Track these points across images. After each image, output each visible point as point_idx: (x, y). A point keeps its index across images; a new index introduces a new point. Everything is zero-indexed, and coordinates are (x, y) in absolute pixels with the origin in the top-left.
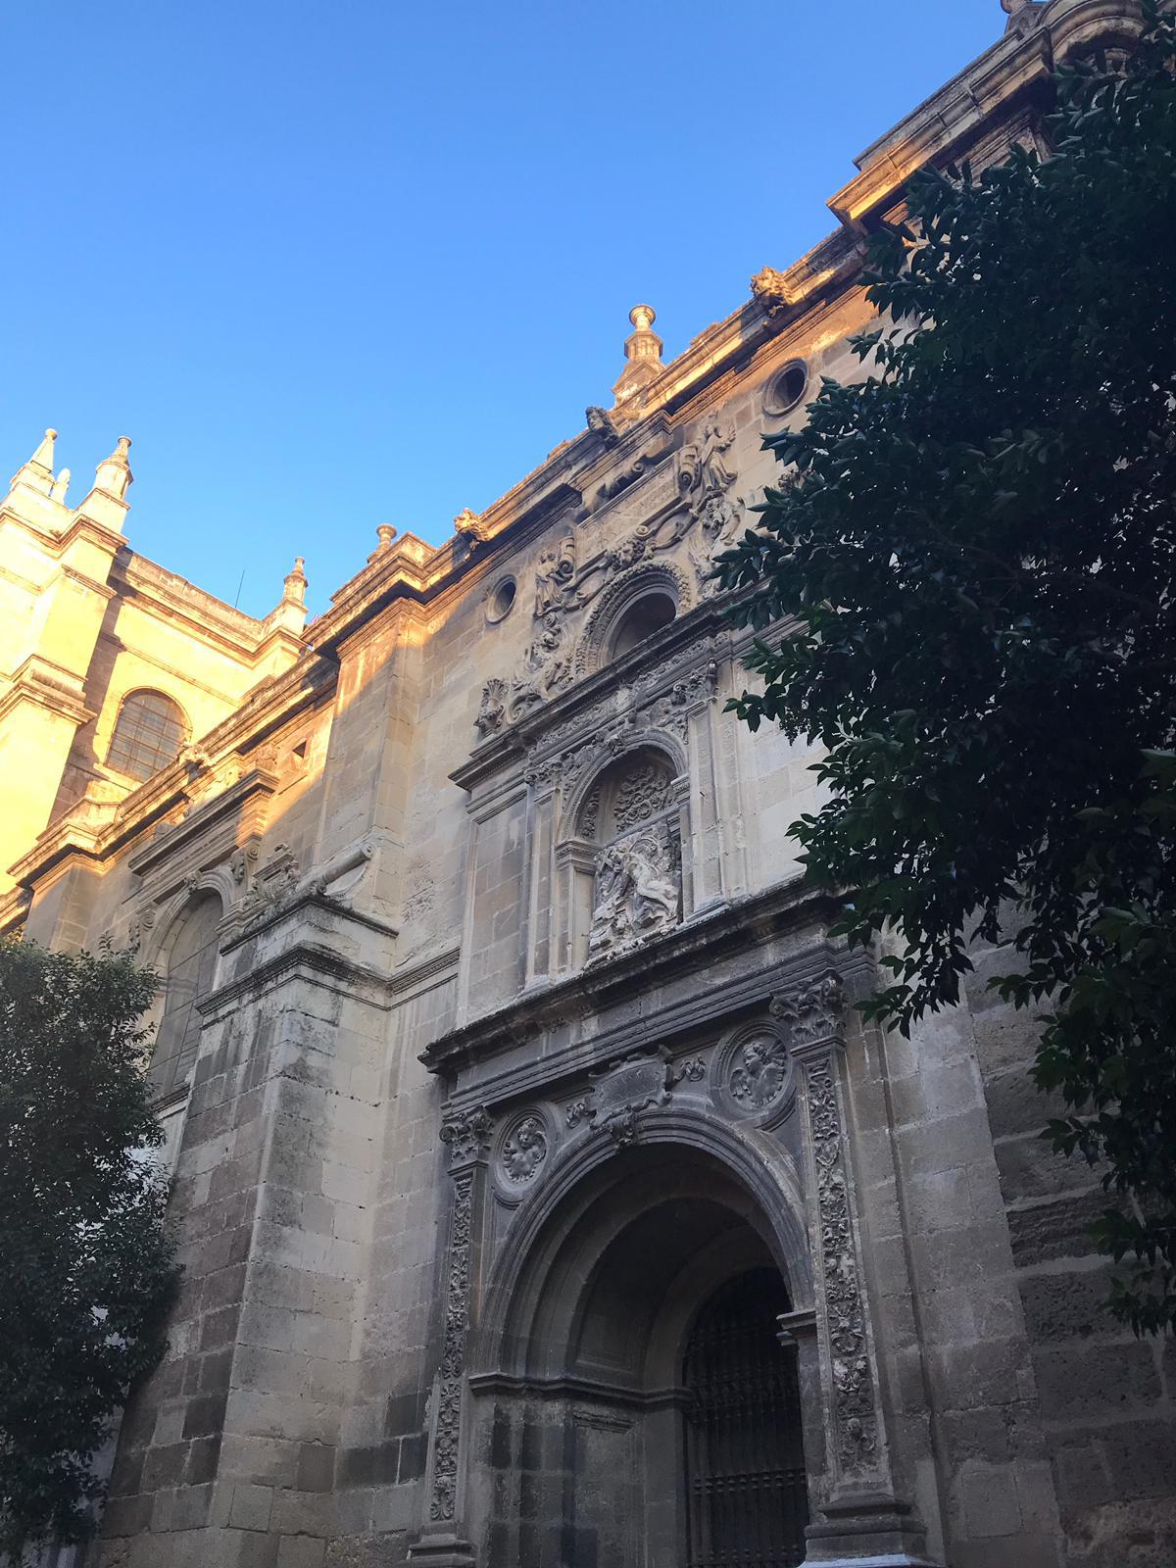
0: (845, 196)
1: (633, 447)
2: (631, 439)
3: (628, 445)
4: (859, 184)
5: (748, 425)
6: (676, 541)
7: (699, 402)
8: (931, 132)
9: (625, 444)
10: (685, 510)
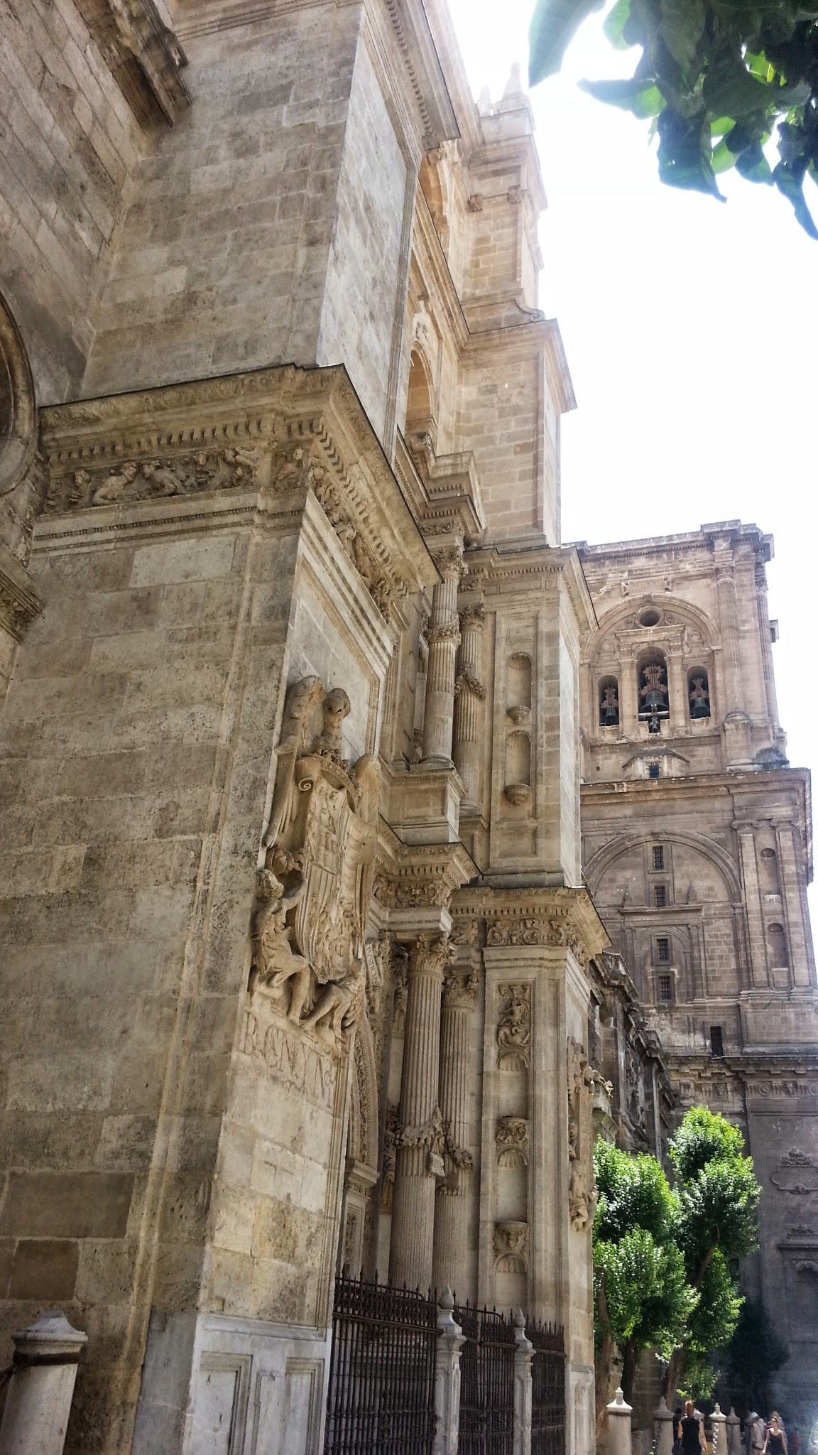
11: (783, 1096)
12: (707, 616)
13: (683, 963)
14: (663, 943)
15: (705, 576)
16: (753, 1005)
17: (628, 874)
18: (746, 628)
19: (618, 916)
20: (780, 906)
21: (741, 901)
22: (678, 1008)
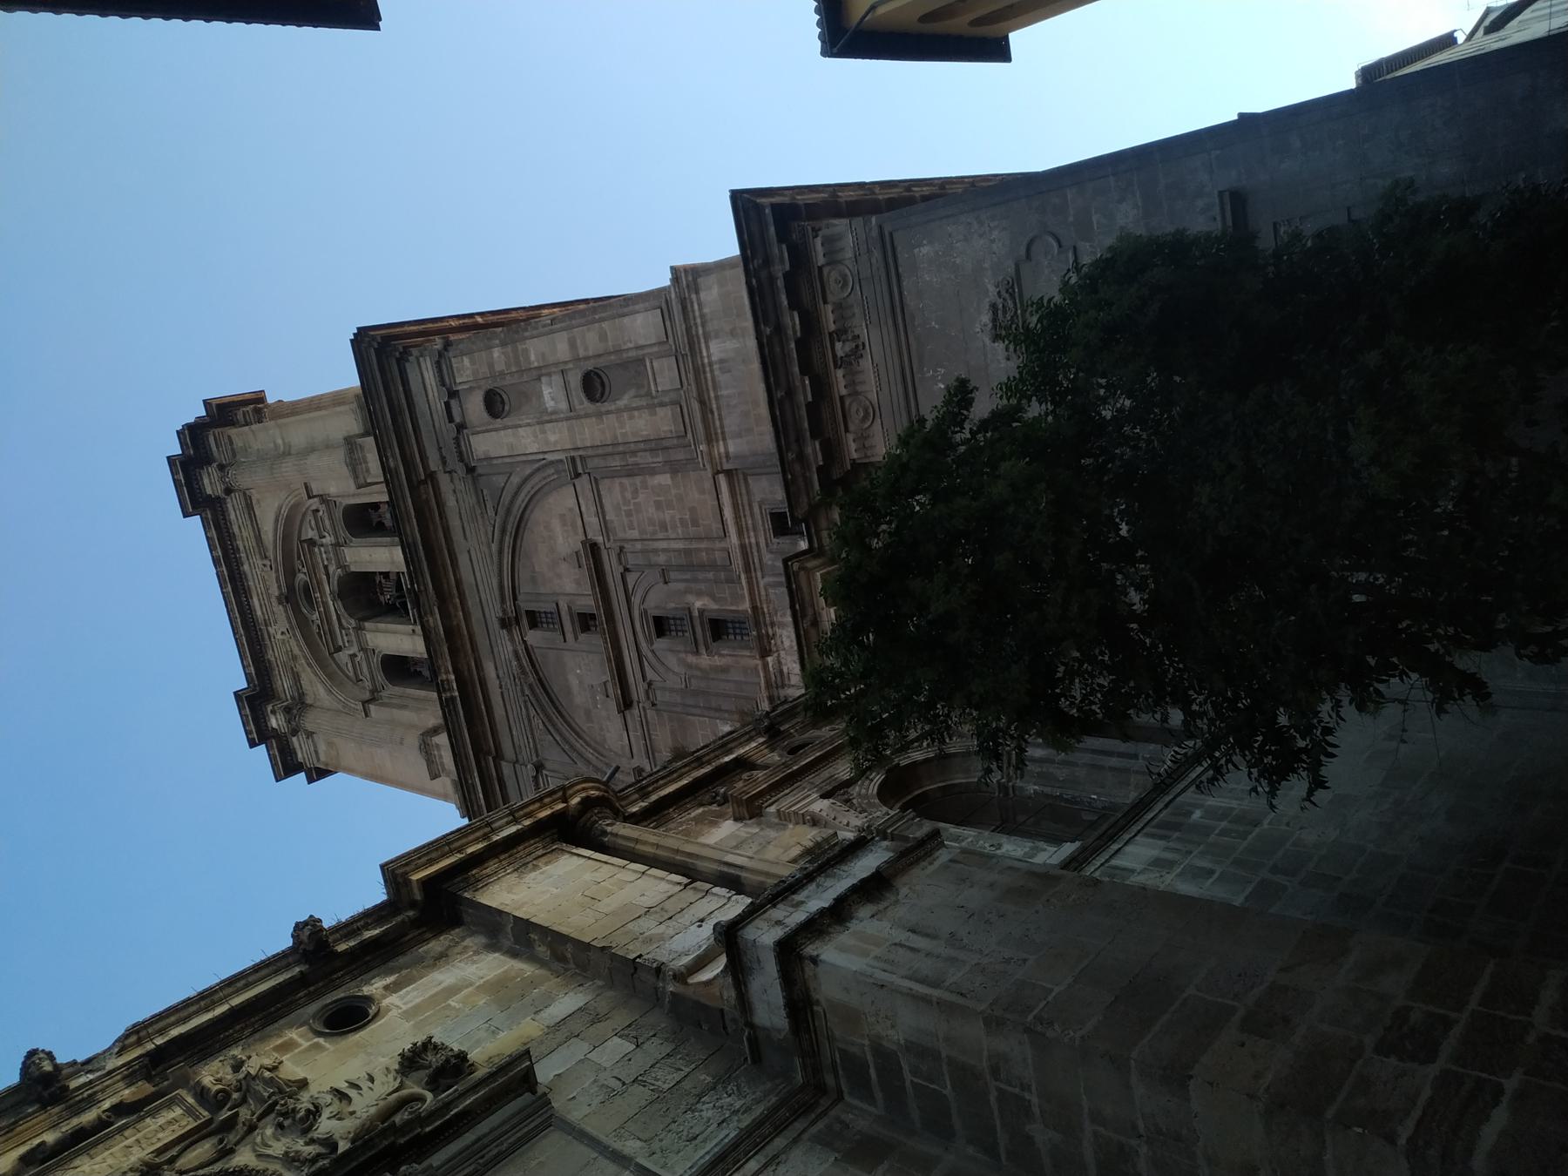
0: (406, 864)
1: (91, 1101)
2: (90, 1092)
3: (83, 1099)
4: (419, 858)
5: (296, 1051)
6: (226, 1153)
7: (202, 1050)
8: (478, 834)
9: (77, 1099)
10: (230, 1124)
11: (866, 364)
12: (280, 508)
13: (681, 586)
14: (661, 626)
15: (249, 507)
16: (710, 440)
17: (574, 682)
18: (280, 441)
19: (636, 711)
20: (554, 378)
21: (561, 461)
22: (754, 608)
